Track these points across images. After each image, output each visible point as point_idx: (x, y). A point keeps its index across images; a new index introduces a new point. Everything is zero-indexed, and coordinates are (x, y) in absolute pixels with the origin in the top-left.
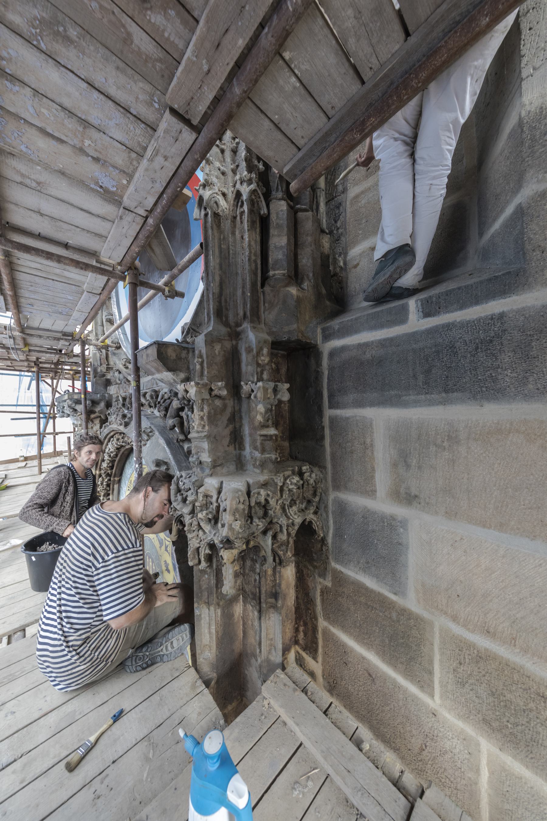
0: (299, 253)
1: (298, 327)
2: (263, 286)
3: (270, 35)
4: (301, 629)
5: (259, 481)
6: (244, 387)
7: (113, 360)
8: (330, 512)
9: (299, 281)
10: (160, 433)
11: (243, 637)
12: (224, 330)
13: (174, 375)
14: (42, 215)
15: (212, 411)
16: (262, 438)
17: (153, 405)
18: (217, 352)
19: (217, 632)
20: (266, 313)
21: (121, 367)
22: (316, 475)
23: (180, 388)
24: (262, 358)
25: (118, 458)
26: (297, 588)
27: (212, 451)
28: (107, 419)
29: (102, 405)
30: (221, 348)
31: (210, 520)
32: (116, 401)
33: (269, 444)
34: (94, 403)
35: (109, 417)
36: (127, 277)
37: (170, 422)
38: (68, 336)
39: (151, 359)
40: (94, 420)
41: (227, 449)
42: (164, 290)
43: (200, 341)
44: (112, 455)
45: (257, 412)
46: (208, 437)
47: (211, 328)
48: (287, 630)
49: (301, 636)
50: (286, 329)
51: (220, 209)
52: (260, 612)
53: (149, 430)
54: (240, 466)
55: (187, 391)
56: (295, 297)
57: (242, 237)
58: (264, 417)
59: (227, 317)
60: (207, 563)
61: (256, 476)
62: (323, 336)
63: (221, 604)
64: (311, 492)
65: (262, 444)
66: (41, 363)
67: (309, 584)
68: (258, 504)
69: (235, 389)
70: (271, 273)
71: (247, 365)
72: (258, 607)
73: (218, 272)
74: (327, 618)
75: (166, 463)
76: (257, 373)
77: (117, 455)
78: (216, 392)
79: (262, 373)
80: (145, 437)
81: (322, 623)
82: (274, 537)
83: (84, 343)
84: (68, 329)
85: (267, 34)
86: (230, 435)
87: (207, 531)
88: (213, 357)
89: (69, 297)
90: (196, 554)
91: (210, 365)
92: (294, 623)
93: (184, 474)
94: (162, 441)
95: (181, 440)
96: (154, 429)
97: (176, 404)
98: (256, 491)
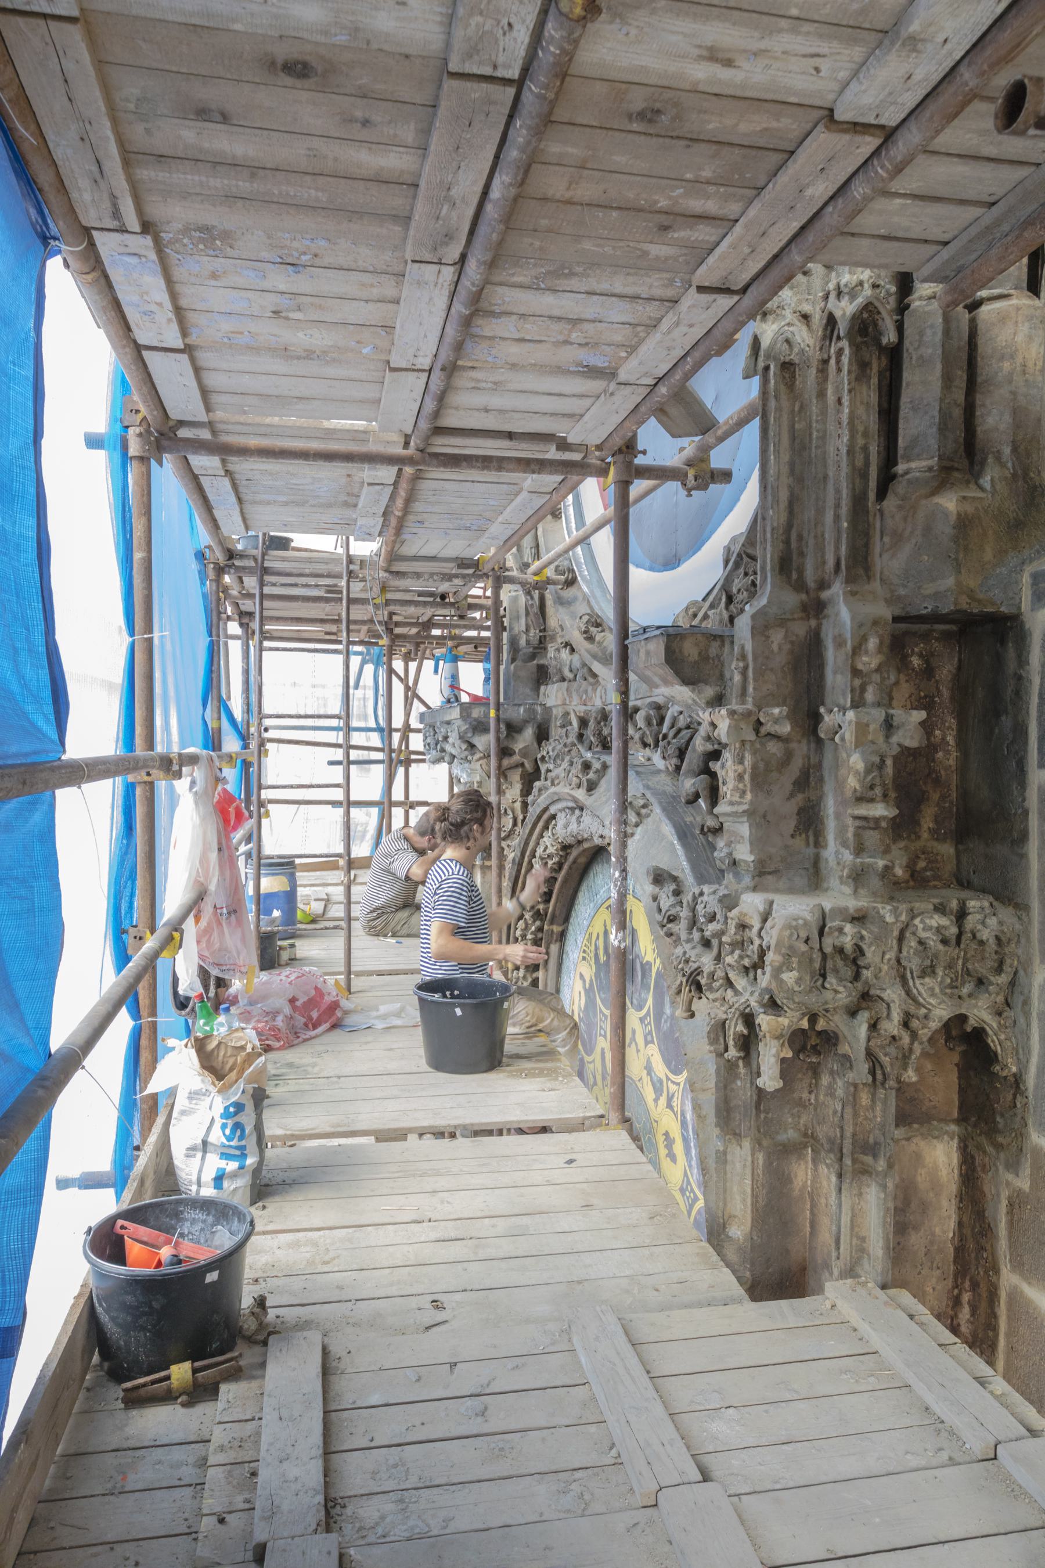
0: (978, 402)
1: (959, 583)
2: (882, 493)
3: (835, 216)
4: (966, 1297)
5: (846, 909)
6: (826, 718)
7: (556, 616)
8: (1034, 1014)
9: (977, 468)
10: (664, 809)
11: (811, 1233)
12: (792, 599)
13: (693, 691)
14: (487, 411)
15: (761, 765)
16: (858, 823)
17: (650, 740)
18: (775, 647)
19: (755, 1196)
20: (886, 556)
21: (577, 638)
22: (1001, 923)
23: (705, 716)
24: (865, 659)
25: (563, 872)
26: (961, 1201)
27: (756, 843)
28: (537, 770)
29: (529, 733)
30: (786, 637)
31: (746, 970)
32: (563, 726)
33: (872, 838)
34: (513, 729)
35: (543, 768)
36: (612, 468)
37: (689, 784)
38: (468, 567)
39: (654, 661)
40: (509, 774)
41: (791, 842)
42: (686, 475)
43: (744, 624)
44: (550, 863)
45: (850, 769)
46: (750, 813)
47: (764, 601)
48: (929, 1290)
49: (965, 1314)
50: (929, 589)
51: (796, 350)
52: (840, 1176)
53: (642, 802)
54: (815, 878)
55: (714, 726)
56: (953, 518)
57: (839, 401)
58: (861, 781)
59: (801, 572)
60: (739, 1050)
61: (838, 896)
62: (1034, 594)
63: (765, 1143)
64: (990, 963)
65: (857, 835)
66: (397, 624)
67: (986, 1189)
68: (840, 951)
69: (809, 720)
70: (901, 468)
71: (835, 673)
72: (837, 1166)
73: (785, 480)
74: (1018, 1265)
75: (675, 879)
76: (853, 690)
77: (560, 865)
78: (769, 727)
79: (863, 689)
80: (632, 818)
81: (1008, 1279)
82: (873, 1026)
83: (499, 579)
84: (466, 554)
85: (831, 213)
86: (798, 814)
87: (739, 988)
88: (767, 658)
89: (492, 502)
90: (721, 1034)
91: (759, 674)
92: (950, 1282)
93: (706, 889)
94: (668, 829)
95: (709, 830)
96: (652, 800)
97: (700, 745)
98: (836, 923)
